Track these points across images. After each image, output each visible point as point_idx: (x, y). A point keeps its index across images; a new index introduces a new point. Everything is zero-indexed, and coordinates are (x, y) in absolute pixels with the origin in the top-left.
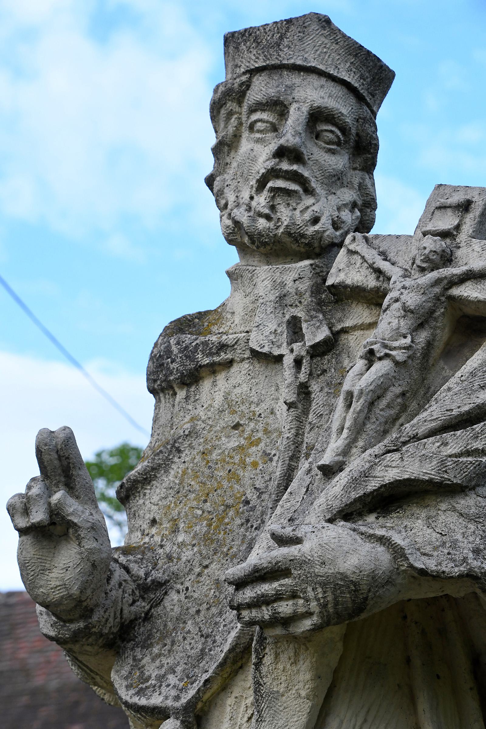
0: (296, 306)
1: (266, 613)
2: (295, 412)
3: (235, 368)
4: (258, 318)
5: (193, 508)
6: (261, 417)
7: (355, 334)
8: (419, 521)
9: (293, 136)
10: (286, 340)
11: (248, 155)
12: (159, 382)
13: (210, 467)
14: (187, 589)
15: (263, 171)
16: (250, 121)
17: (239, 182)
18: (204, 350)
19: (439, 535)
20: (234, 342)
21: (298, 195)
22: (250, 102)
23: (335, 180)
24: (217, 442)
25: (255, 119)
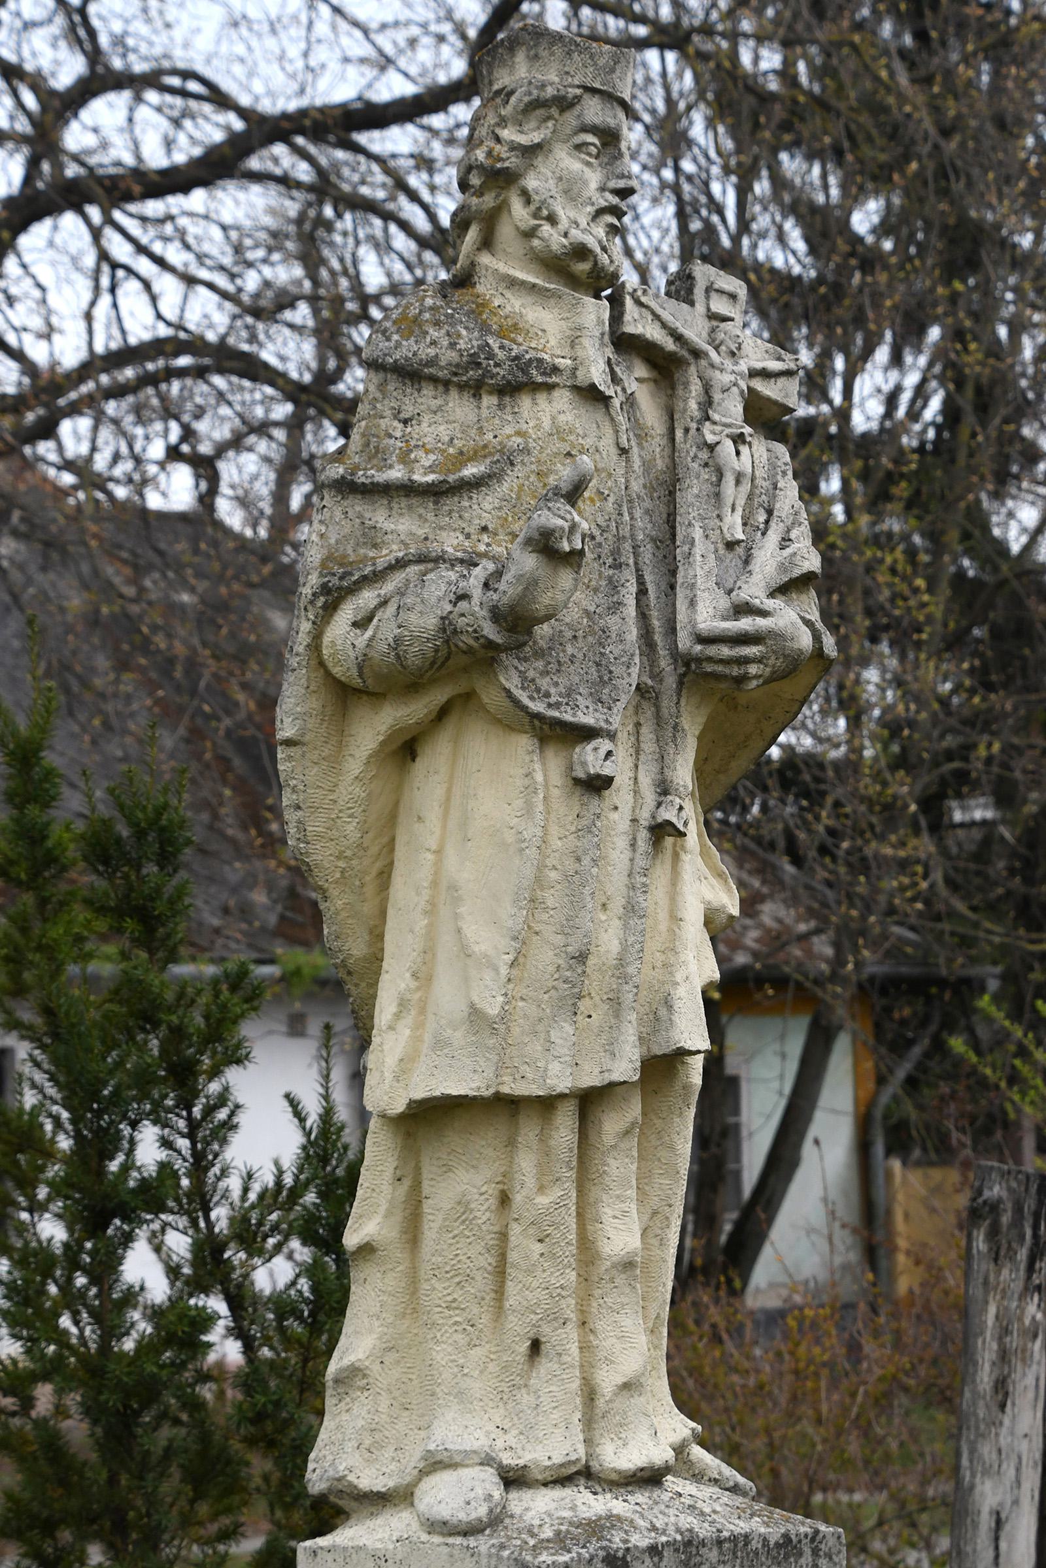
1: (735, 671)
3: (556, 393)
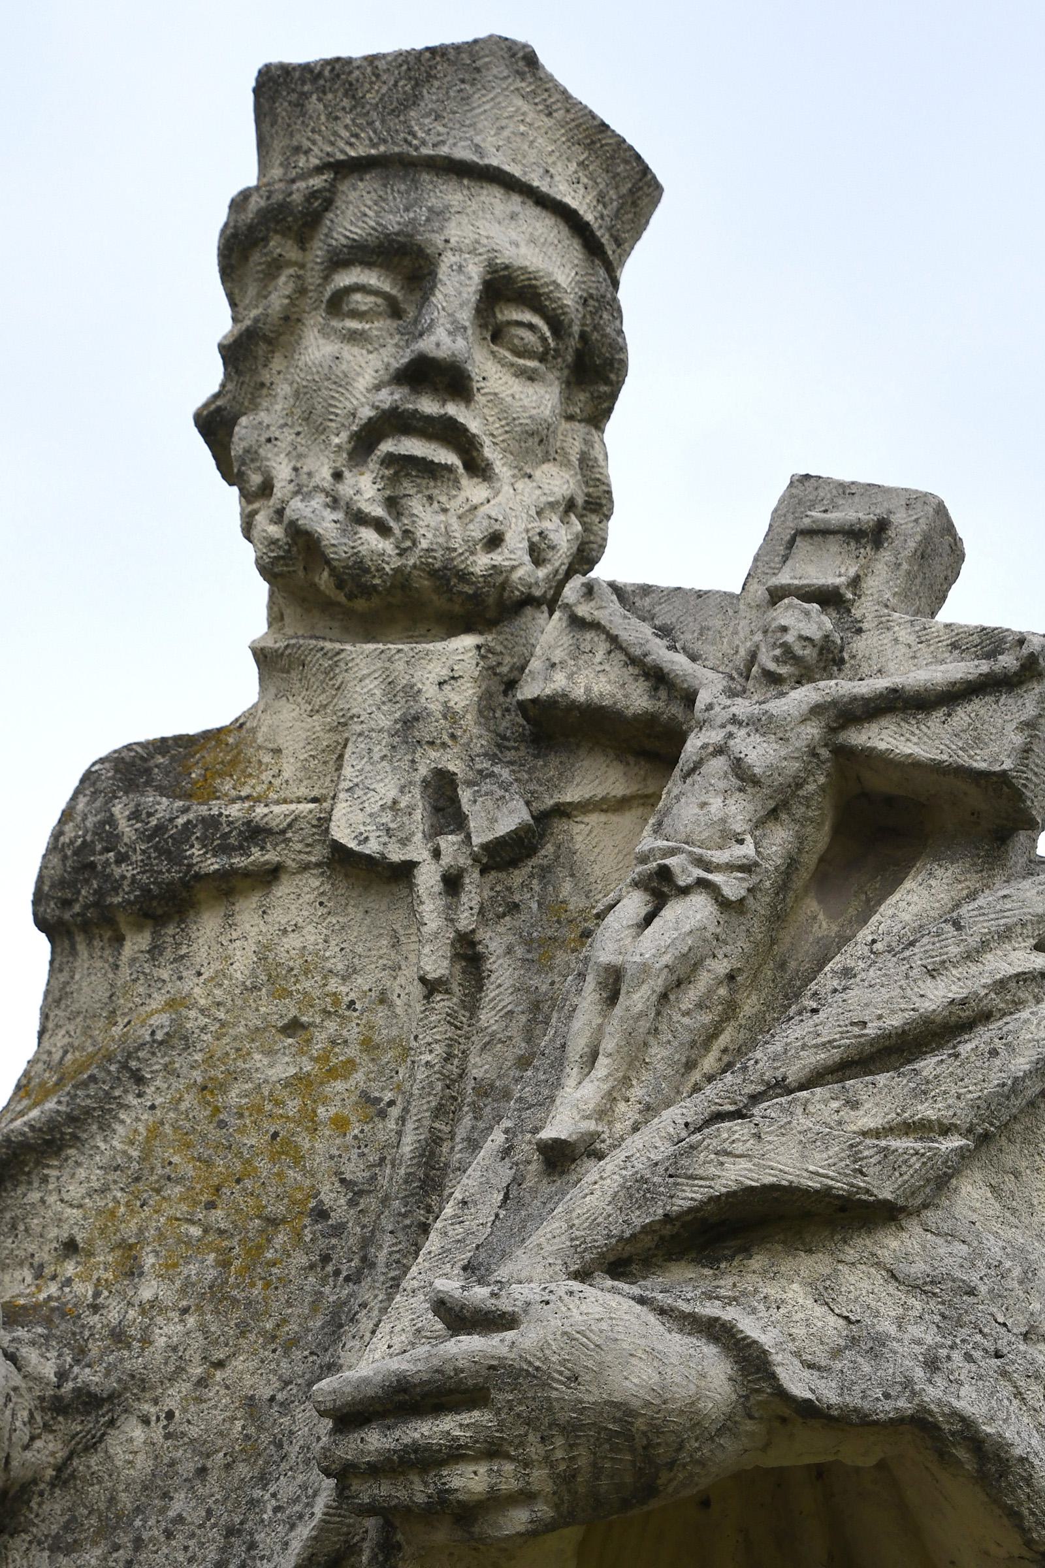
0: (444, 745)
1: (419, 1491)
2: (446, 1003)
3: (283, 889)
4: (350, 769)
5: (177, 1219)
6: (355, 1010)
7: (586, 820)
8: (795, 1286)
9: (450, 333)
10: (421, 828)
11: (326, 371)
12: (77, 908)
13: (222, 1124)
14: (170, 1415)
15: (366, 413)
16: (329, 290)
17: (298, 434)
18: (206, 837)
19: (841, 1322)
20: (285, 824)
21: (452, 476)
22: (334, 243)
23: (535, 443)
24: (240, 1063)
25: (347, 283)
